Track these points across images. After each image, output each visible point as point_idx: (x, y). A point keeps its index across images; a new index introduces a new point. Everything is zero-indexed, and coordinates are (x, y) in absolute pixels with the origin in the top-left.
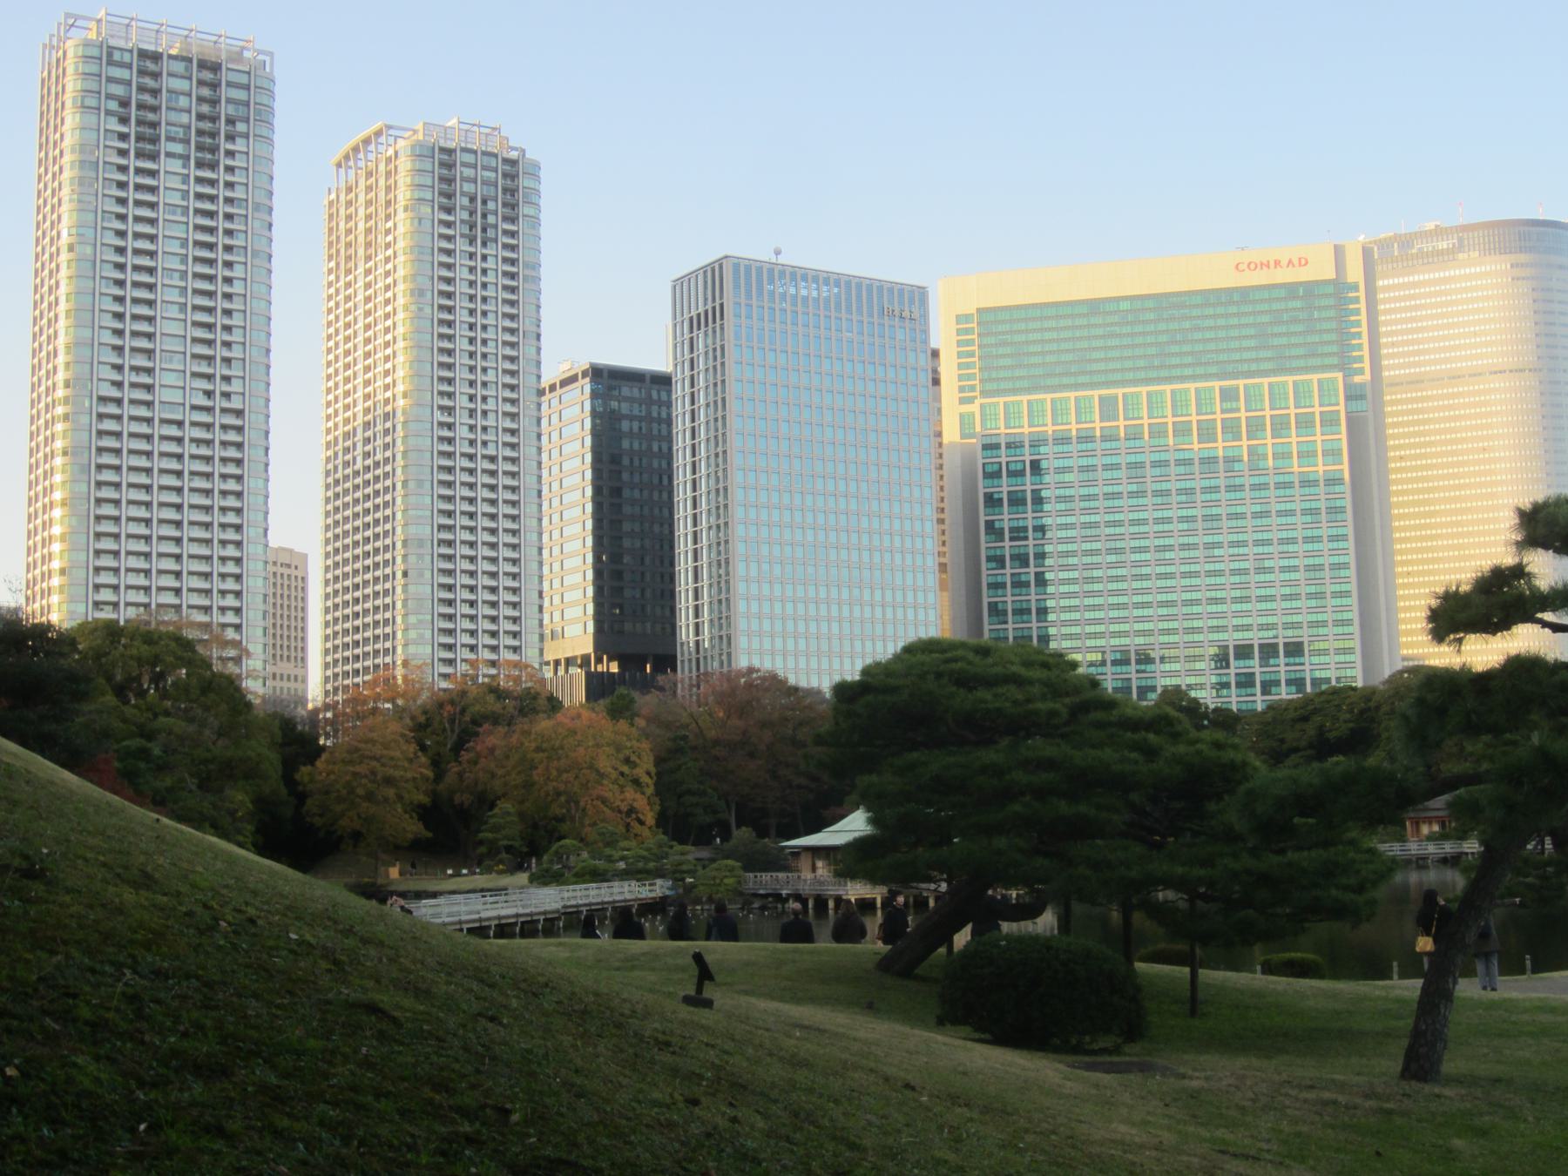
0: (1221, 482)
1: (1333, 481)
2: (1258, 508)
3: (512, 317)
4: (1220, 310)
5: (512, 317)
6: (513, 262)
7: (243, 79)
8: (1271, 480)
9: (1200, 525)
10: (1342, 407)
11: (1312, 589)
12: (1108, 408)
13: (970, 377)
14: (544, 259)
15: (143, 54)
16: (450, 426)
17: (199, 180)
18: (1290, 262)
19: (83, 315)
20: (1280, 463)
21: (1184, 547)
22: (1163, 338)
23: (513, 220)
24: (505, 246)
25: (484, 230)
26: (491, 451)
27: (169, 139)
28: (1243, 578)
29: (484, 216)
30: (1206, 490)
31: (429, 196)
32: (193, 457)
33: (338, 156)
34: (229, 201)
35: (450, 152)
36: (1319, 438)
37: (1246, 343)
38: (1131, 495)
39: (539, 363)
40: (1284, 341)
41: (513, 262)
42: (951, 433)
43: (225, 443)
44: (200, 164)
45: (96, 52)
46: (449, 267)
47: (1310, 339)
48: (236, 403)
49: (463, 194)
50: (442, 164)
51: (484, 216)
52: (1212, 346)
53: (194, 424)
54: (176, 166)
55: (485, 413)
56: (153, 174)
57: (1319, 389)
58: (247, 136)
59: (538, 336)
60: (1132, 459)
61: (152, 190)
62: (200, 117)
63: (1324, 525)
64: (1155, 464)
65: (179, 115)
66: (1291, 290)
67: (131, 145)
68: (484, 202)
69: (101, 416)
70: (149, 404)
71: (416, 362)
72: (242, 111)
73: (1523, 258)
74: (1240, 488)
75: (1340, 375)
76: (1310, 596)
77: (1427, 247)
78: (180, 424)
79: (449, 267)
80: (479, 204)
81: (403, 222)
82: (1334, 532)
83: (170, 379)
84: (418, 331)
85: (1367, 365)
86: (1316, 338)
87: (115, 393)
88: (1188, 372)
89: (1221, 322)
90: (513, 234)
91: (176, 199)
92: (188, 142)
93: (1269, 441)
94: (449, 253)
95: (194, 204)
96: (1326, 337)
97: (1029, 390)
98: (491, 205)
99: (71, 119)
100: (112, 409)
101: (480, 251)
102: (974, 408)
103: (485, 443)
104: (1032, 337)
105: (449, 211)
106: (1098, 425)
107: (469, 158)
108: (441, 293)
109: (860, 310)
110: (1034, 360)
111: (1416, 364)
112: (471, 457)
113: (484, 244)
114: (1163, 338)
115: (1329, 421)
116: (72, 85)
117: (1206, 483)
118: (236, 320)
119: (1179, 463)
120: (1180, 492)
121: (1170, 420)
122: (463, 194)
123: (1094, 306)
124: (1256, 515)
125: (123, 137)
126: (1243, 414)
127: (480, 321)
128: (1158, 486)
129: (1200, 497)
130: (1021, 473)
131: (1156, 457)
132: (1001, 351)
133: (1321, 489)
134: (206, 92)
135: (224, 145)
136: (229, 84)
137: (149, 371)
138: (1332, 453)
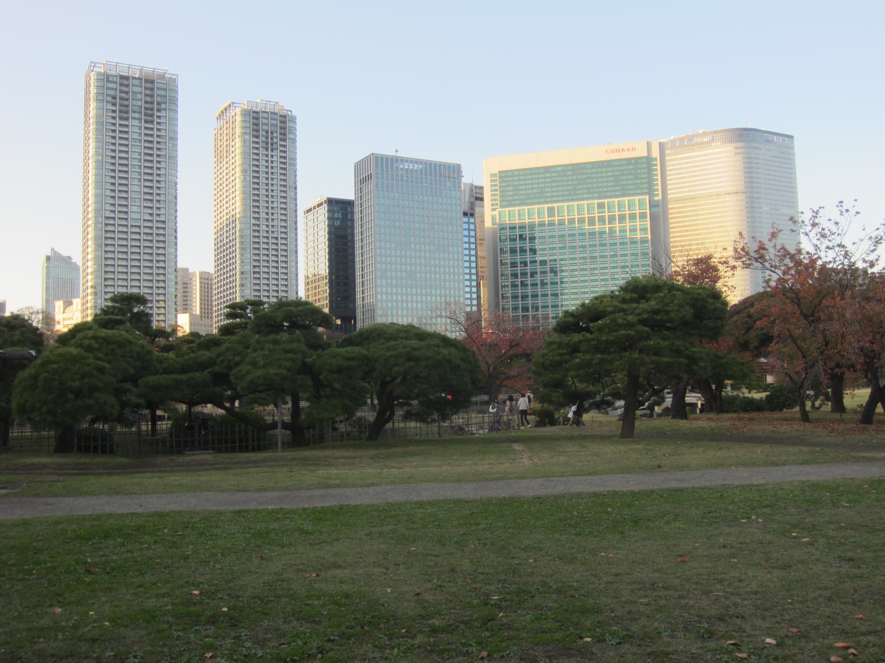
0: (597, 243)
1: (644, 241)
2: (612, 253)
3: (285, 180)
4: (599, 170)
5: (285, 180)
6: (285, 158)
7: (164, 86)
8: (618, 241)
9: (588, 261)
10: (648, 211)
12: (551, 211)
13: (495, 200)
14: (298, 156)
15: (122, 77)
16: (258, 225)
17: (146, 128)
19: (99, 184)
20: (622, 234)
21: (581, 270)
22: (575, 182)
23: (285, 140)
24: (281, 151)
25: (272, 145)
26: (275, 235)
27: (133, 112)
28: (607, 283)
29: (272, 139)
30: (590, 246)
31: (248, 131)
32: (144, 240)
33: (217, 115)
34: (158, 136)
35: (257, 113)
36: (638, 223)
37: (609, 184)
38: (560, 248)
39: (296, 199)
40: (625, 182)
41: (285, 158)
42: (488, 224)
43: (160, 233)
44: (146, 122)
45: (102, 77)
46: (258, 160)
47: (637, 181)
48: (162, 218)
49: (263, 130)
50: (254, 118)
51: (272, 139)
52: (595, 185)
53: (144, 227)
54: (136, 123)
55: (273, 220)
56: (127, 126)
57: (639, 202)
58: (165, 110)
59: (296, 188)
60: (560, 233)
61: (127, 132)
62: (146, 102)
64: (570, 235)
65: (137, 102)
66: (629, 161)
67: (117, 115)
68: (272, 133)
69: (106, 225)
70: (126, 219)
71: (244, 199)
72: (163, 100)
73: (739, 144)
74: (605, 245)
75: (647, 197)
77: (699, 140)
78: (139, 227)
79: (258, 160)
80: (269, 136)
81: (238, 143)
83: (135, 209)
84: (244, 187)
85: (660, 192)
86: (638, 181)
87: (112, 215)
88: (586, 196)
89: (600, 175)
90: (285, 146)
91: (136, 136)
92: (141, 113)
93: (617, 225)
94: (257, 154)
95: (143, 138)
96: (644, 181)
97: (520, 205)
98: (275, 135)
99: (93, 105)
100: (112, 222)
101: (270, 153)
102: (496, 213)
103: (273, 232)
104: (521, 183)
105: (257, 137)
106: (547, 219)
107: (265, 115)
108: (254, 171)
109: (431, 174)
110: (522, 192)
111: (708, 189)
112: (267, 238)
113: (272, 150)
114: (575, 182)
115: (643, 216)
116: (93, 91)
117: (591, 243)
118: (162, 185)
119: (580, 234)
120: (580, 247)
121: (576, 217)
122: (263, 130)
123: (547, 169)
124: (611, 256)
125: (114, 111)
126: (607, 214)
127: (270, 182)
128: (571, 245)
129: (588, 249)
130: (515, 240)
131: (570, 232)
132: (509, 189)
133: (639, 245)
134: (148, 92)
135: (156, 113)
136: (158, 89)
137: (126, 206)
138: (644, 230)
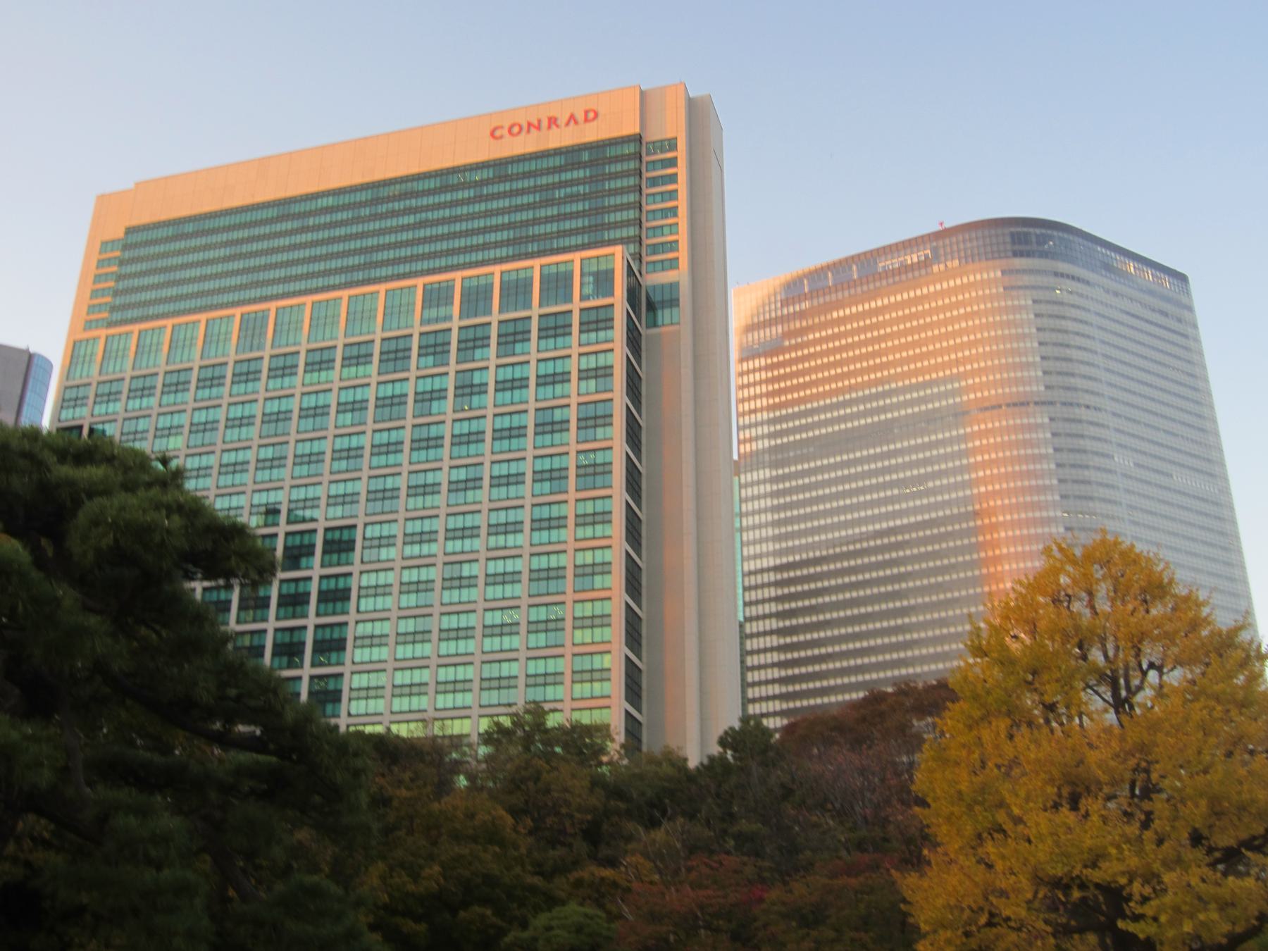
11: (542, 614)
12: (252, 329)
18: (572, 117)
28: (423, 598)
30: (377, 450)
63: (572, 495)
66: (571, 156)
76: (535, 627)
77: (894, 263)
82: (589, 508)
85: (683, 254)
115: (597, 321)
